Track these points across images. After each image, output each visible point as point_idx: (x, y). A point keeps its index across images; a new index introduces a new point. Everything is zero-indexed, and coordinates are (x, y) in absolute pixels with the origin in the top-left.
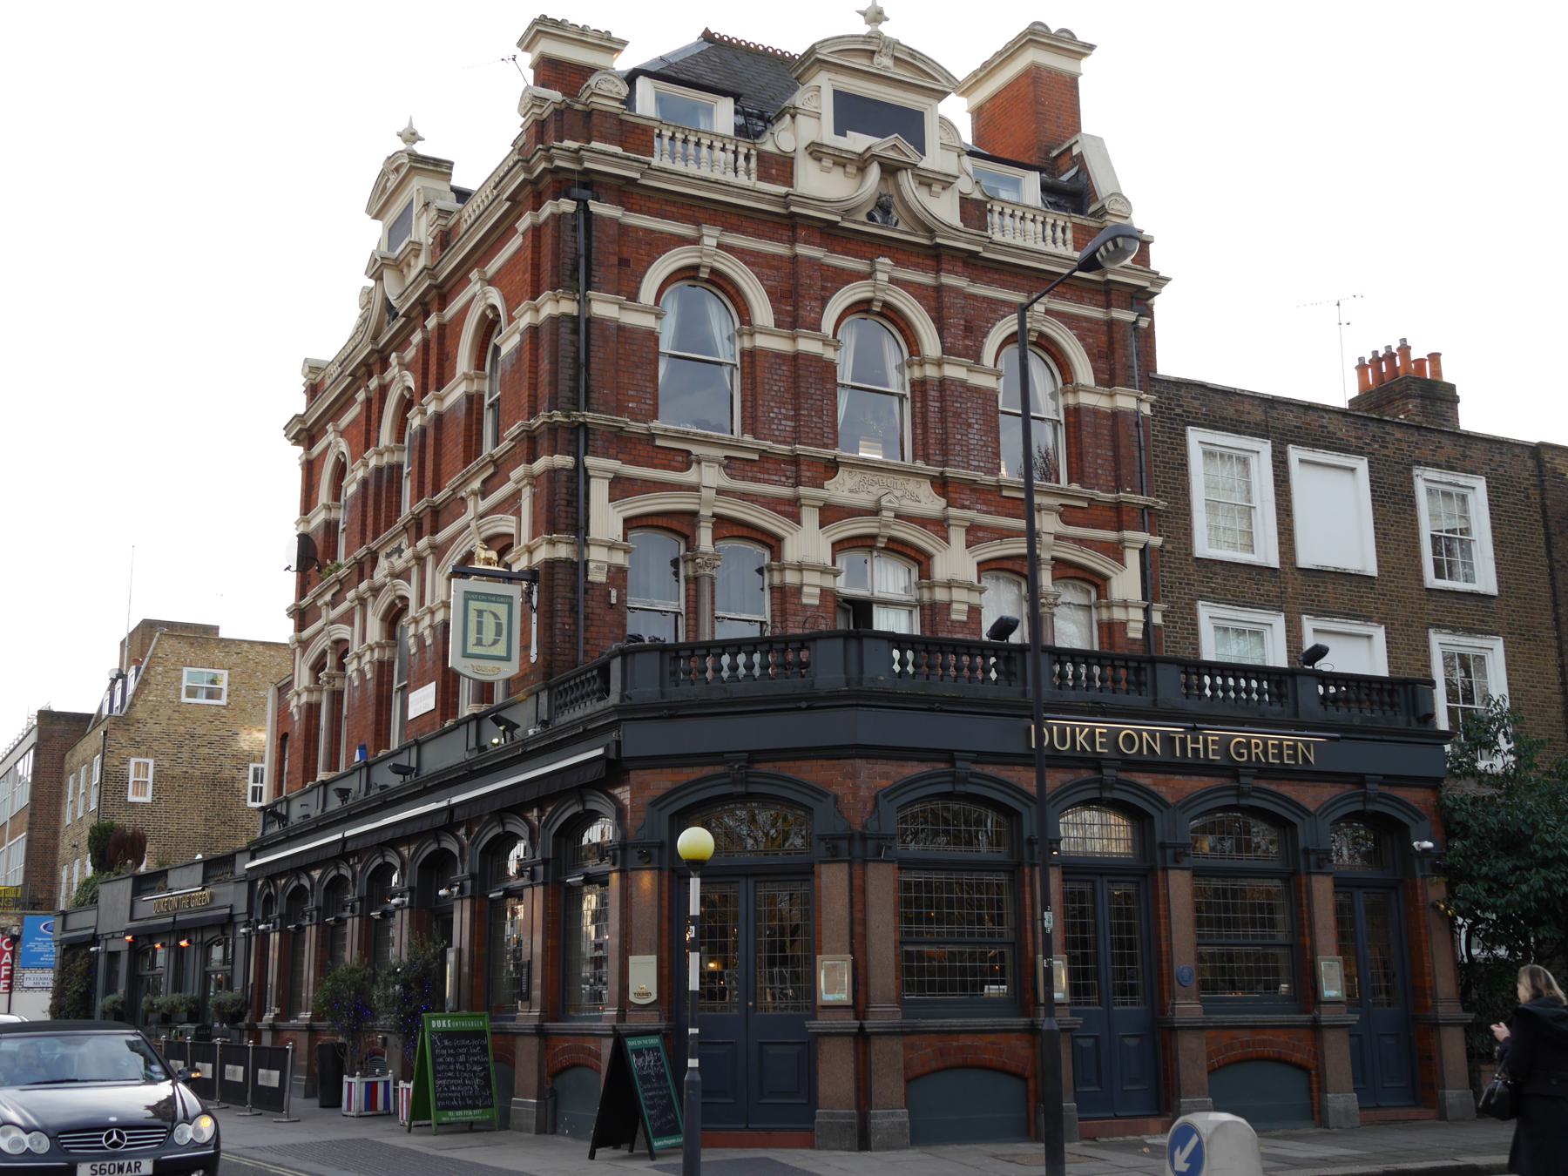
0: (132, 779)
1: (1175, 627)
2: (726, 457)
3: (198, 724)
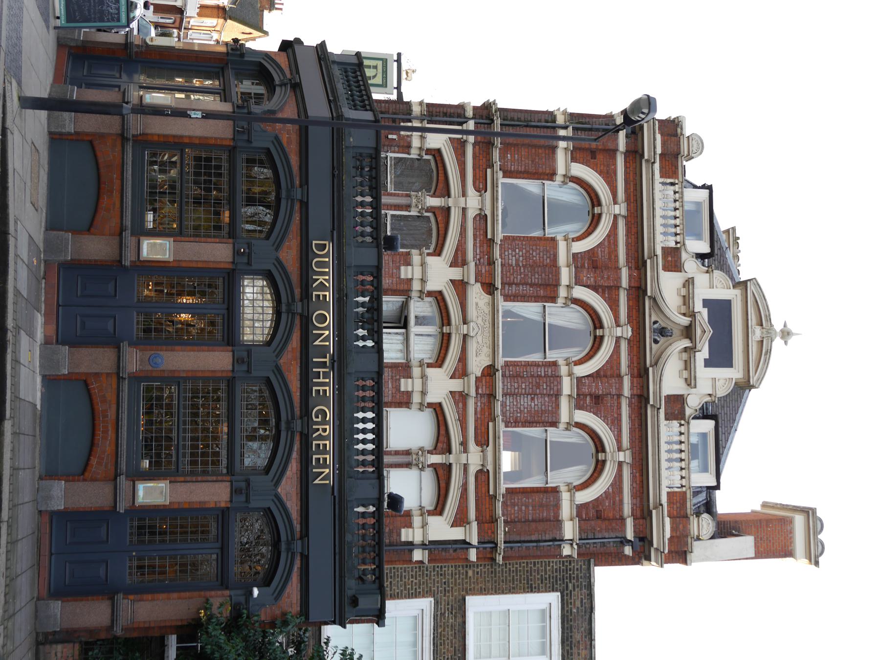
1: (412, 578)
2: (486, 215)
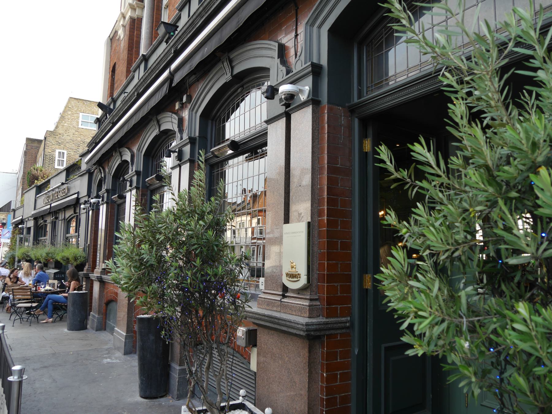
0: (57, 158)
3: (86, 137)
